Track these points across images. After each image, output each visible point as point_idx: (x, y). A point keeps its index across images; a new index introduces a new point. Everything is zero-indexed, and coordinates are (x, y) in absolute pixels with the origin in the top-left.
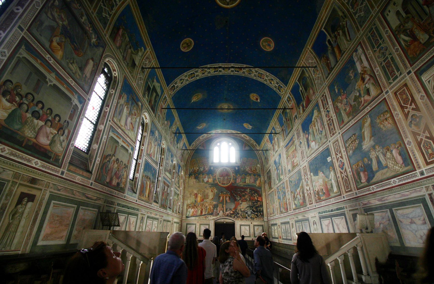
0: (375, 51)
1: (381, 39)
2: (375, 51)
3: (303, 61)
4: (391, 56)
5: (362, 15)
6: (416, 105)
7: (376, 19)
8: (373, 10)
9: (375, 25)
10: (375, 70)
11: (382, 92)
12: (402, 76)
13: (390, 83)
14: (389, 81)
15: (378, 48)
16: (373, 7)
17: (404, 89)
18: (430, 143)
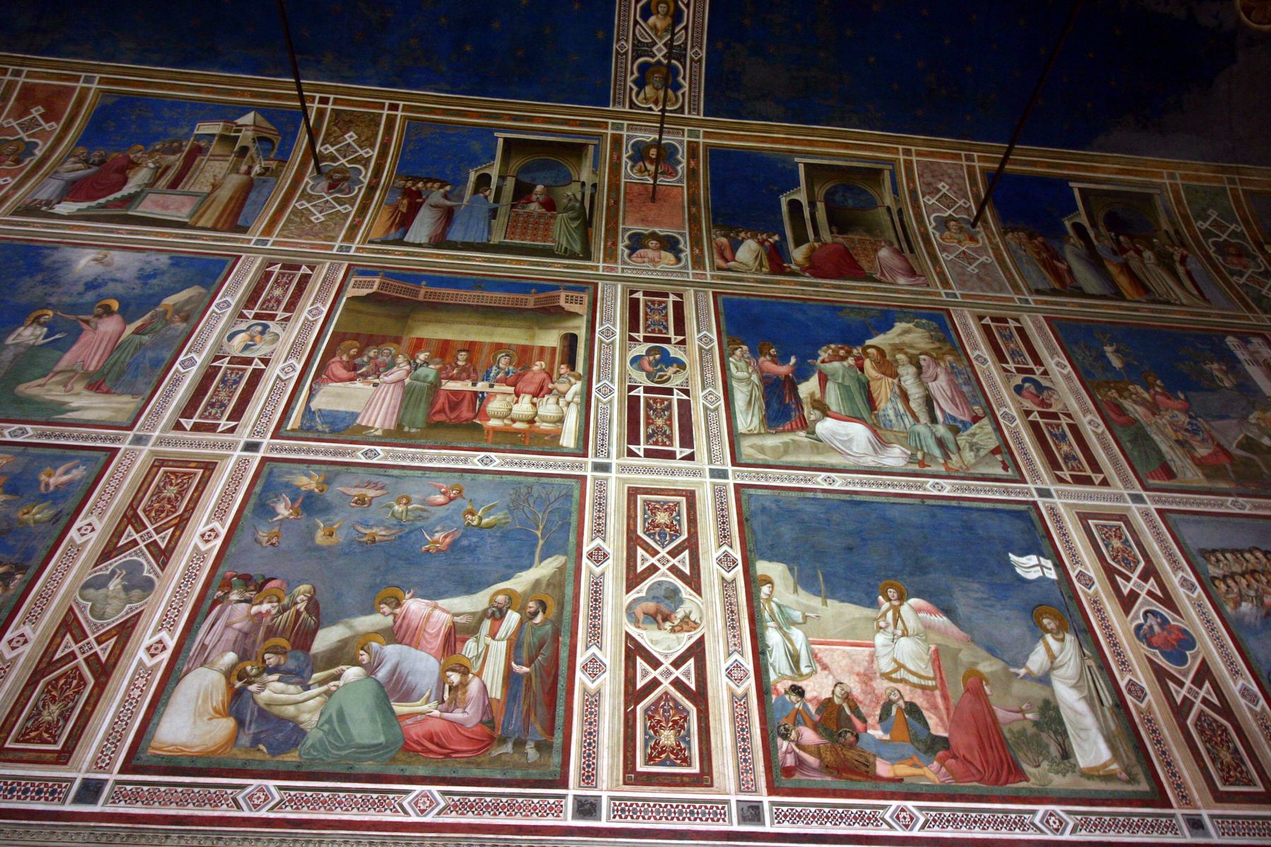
0: (242, 316)
1: (285, 310)
2: (242, 316)
3: (18, 73)
4: (263, 367)
5: (313, 219)
6: (174, 541)
7: (346, 264)
8: (343, 241)
9: (312, 269)
10: (186, 354)
11: (131, 428)
12: (228, 437)
13: (178, 427)
14: (183, 416)
15: (257, 316)
16: (350, 237)
17: (195, 474)
18: (85, 684)
